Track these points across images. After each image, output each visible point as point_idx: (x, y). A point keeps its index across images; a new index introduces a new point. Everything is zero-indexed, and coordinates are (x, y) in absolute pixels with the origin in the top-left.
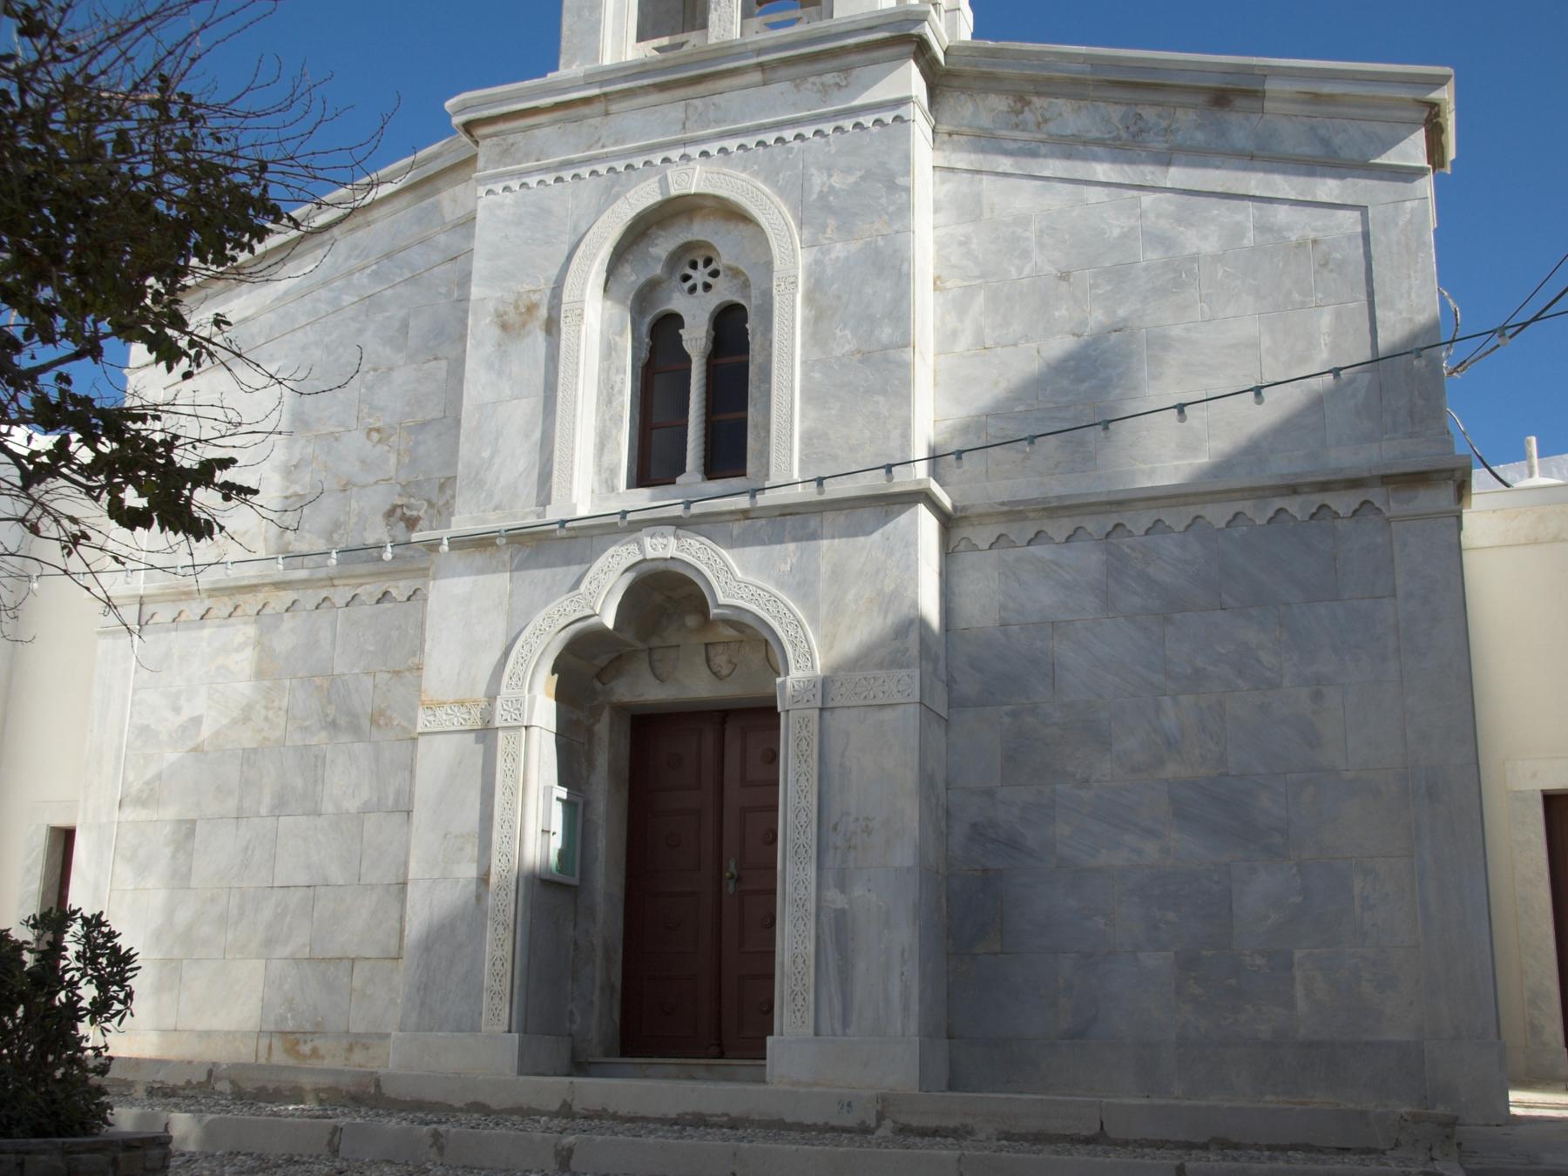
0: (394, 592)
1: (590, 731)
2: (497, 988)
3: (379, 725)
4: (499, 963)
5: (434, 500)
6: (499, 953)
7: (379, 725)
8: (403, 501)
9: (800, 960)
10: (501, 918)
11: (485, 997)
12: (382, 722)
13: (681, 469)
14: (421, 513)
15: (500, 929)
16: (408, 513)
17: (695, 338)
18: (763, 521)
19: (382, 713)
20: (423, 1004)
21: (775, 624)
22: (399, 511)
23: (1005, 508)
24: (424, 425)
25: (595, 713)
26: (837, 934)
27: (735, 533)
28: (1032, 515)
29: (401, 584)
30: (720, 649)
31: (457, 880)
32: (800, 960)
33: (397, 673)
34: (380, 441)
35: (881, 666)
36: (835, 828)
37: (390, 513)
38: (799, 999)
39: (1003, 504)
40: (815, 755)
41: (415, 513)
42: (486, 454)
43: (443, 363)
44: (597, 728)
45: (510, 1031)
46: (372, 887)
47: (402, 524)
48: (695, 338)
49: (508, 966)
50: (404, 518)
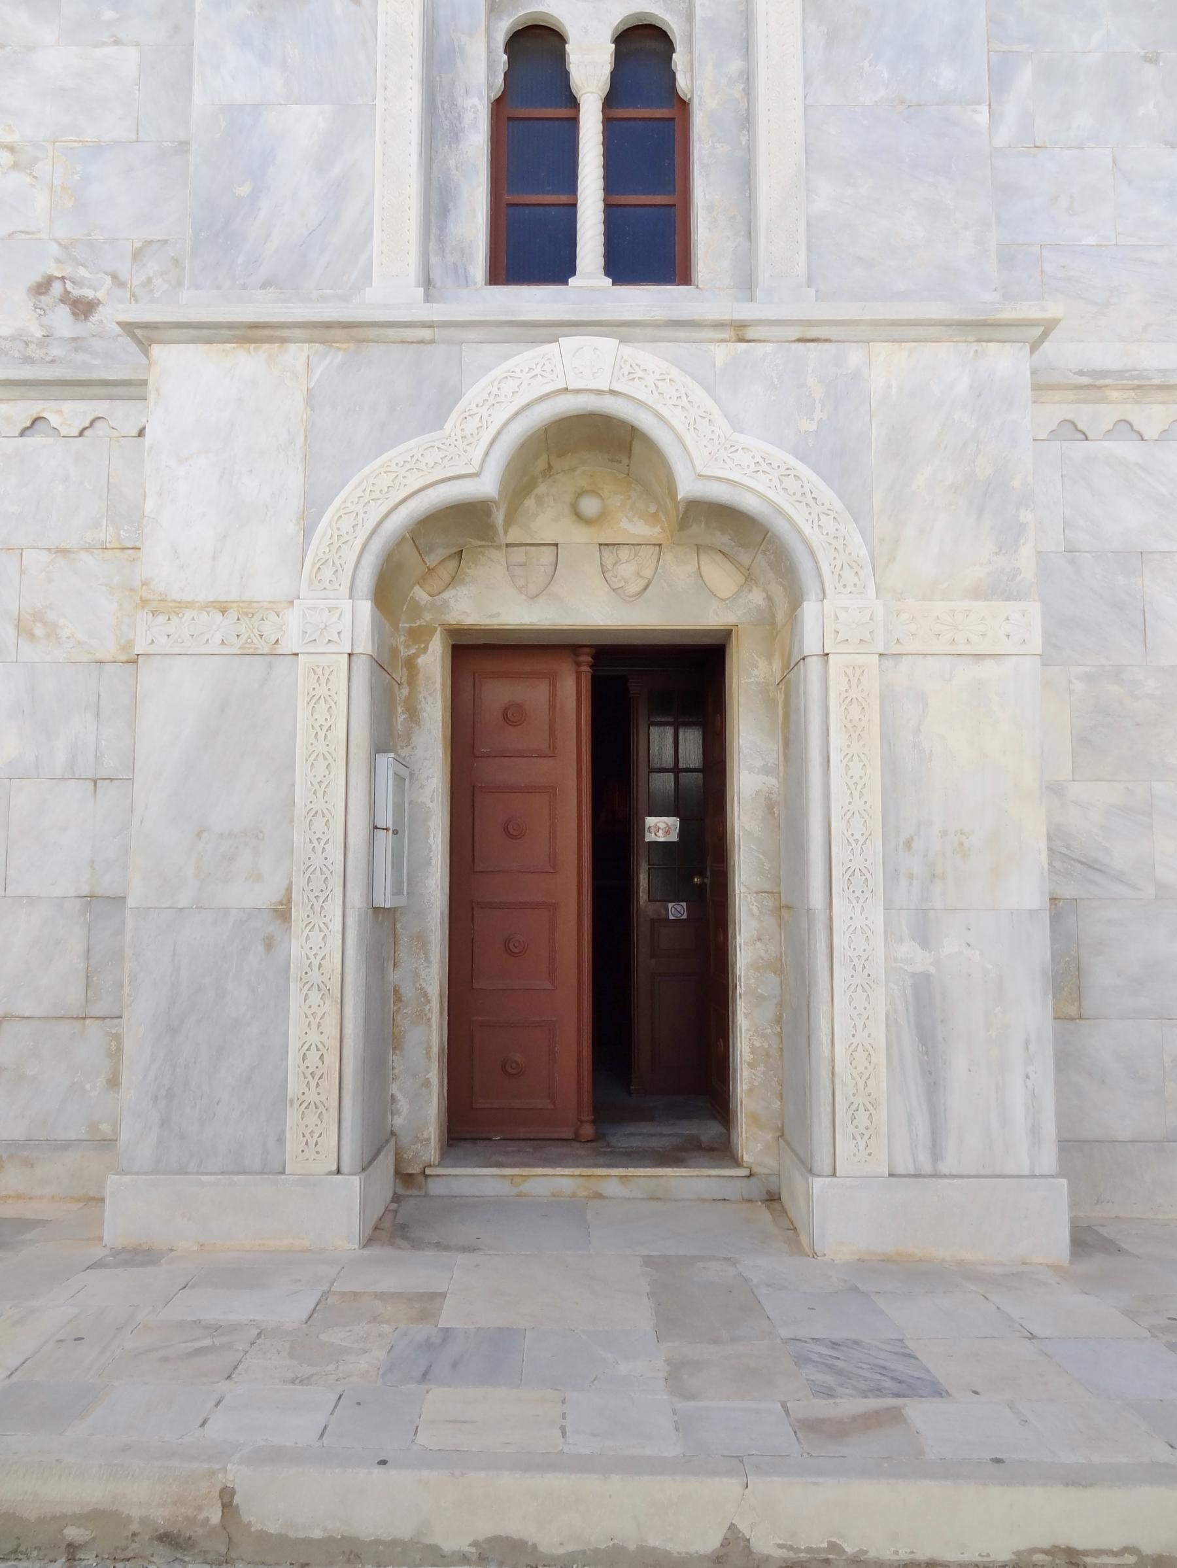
0: (54, 420)
1: (410, 664)
2: (312, 1096)
3: (32, 636)
4: (313, 1055)
5: (124, 275)
6: (314, 1038)
7: (32, 636)
8: (68, 271)
9: (860, 1055)
10: (315, 977)
11: (292, 1116)
12: (39, 630)
13: (572, 270)
14: (100, 295)
15: (315, 997)
16: (76, 292)
17: (590, 68)
18: (768, 347)
19: (38, 617)
20: (164, 1123)
21: (799, 516)
22: (57, 288)
23: (1085, 380)
24: (98, 148)
25: (419, 636)
26: (924, 1015)
27: (719, 362)
28: (1114, 395)
29: (68, 406)
30: (624, 553)
31: (226, 910)
32: (860, 1055)
33: (63, 552)
34: (15, 166)
35: (977, 593)
36: (908, 845)
37: (42, 287)
38: (862, 1116)
39: (1081, 373)
40: (876, 729)
41: (89, 293)
42: (244, 190)
43: (132, 53)
44: (421, 660)
45: (338, 1172)
46: (31, 901)
47: (64, 311)
48: (590, 68)
49: (332, 1059)
50: (66, 298)
